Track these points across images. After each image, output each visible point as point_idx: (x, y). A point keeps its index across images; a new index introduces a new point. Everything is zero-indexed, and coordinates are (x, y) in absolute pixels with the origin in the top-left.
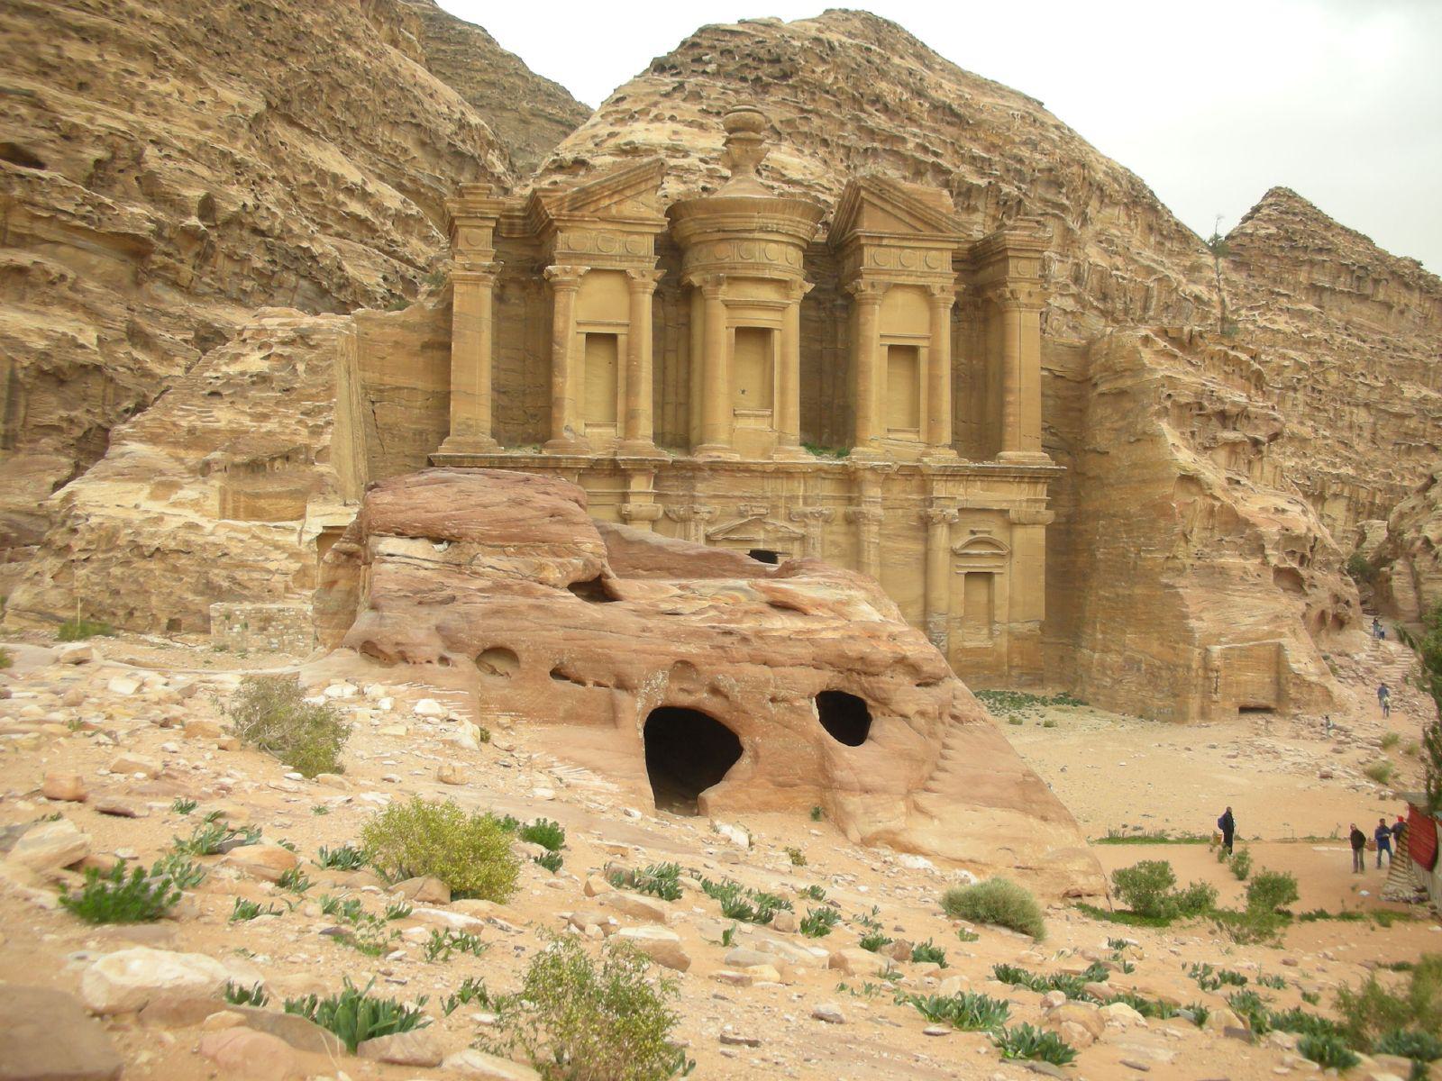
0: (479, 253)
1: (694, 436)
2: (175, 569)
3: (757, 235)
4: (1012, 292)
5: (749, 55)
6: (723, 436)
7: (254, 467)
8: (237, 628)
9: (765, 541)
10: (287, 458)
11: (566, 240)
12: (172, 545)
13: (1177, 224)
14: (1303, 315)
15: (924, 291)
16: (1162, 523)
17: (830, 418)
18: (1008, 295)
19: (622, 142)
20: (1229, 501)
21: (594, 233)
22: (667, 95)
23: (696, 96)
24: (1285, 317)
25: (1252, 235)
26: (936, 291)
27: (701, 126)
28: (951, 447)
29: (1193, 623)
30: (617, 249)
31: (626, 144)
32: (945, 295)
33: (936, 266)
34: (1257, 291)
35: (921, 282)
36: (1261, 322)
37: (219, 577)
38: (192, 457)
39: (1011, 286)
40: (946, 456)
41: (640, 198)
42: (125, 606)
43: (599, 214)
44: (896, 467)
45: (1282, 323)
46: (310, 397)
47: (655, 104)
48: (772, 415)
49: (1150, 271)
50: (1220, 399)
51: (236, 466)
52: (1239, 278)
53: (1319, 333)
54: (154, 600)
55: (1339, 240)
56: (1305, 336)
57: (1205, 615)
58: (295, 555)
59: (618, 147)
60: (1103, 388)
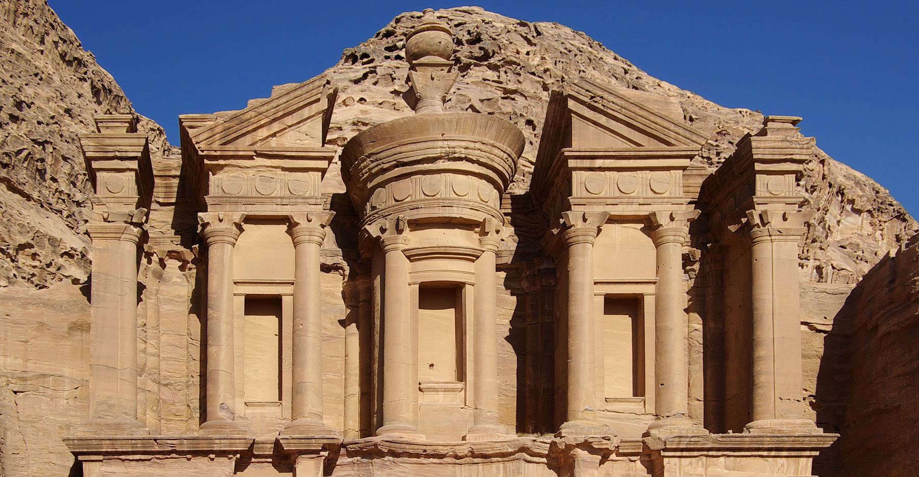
0: (120, 200)
3: (441, 165)
4: (761, 216)
11: (218, 182)
15: (650, 225)
18: (757, 220)
21: (251, 172)
26: (663, 220)
30: (278, 191)
32: (674, 225)
33: (671, 195)
35: (644, 211)
39: (759, 209)
41: (304, 127)
43: (256, 147)
44: (615, 442)
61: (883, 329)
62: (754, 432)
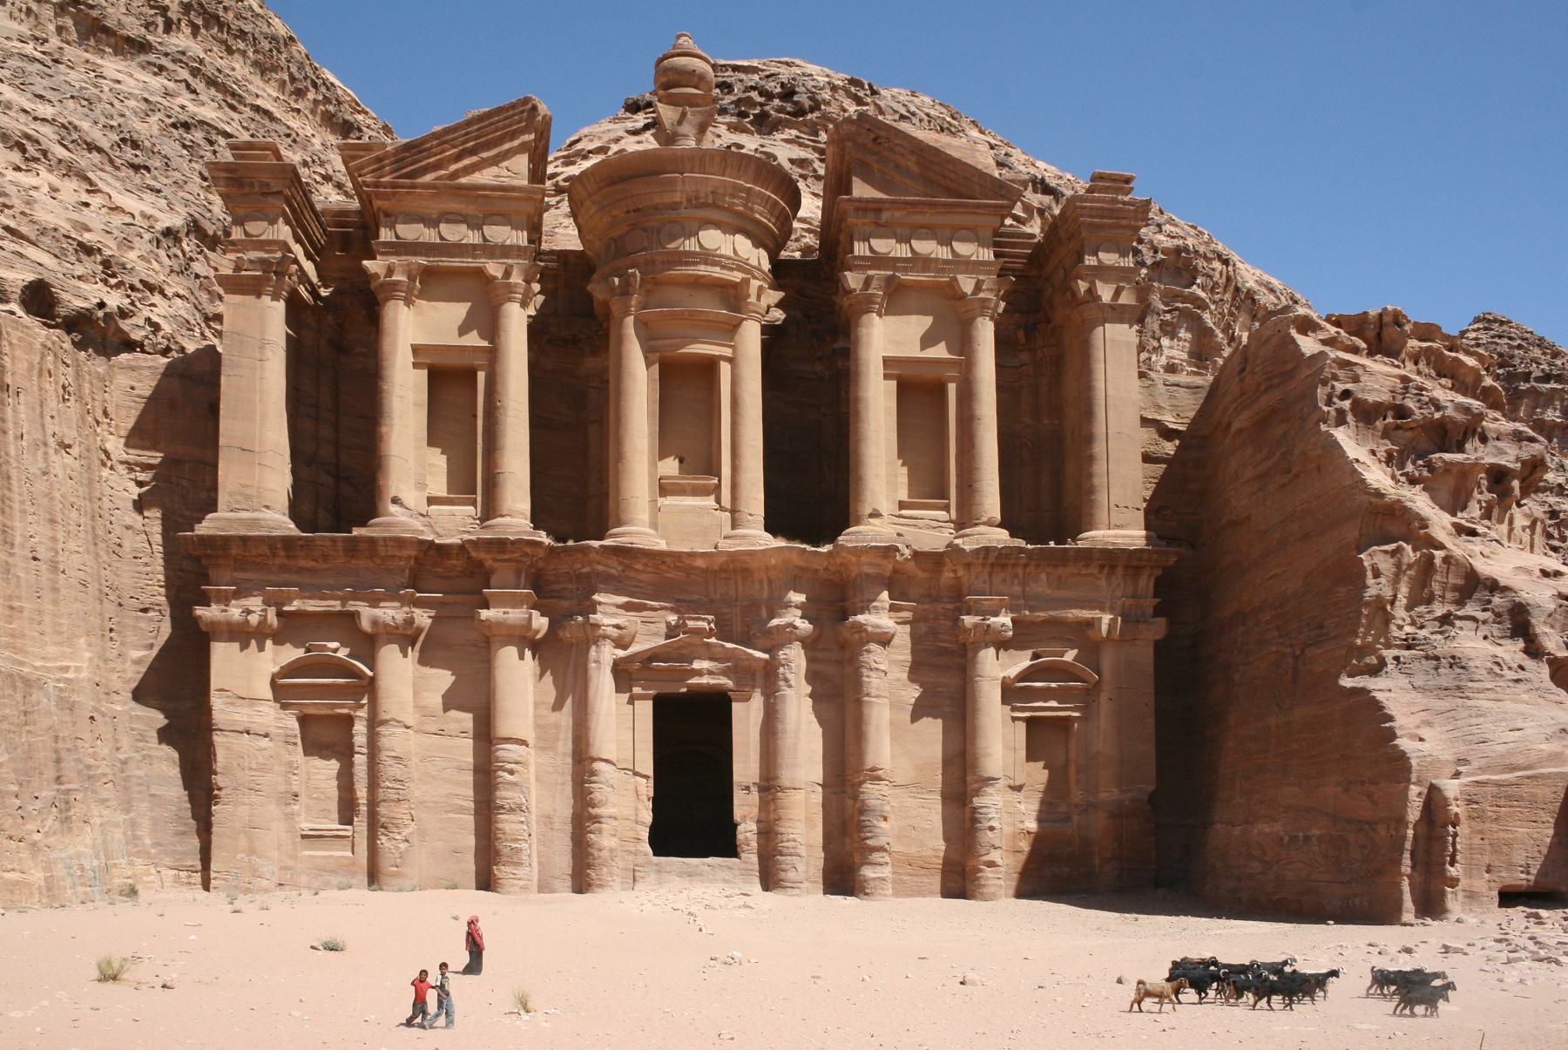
1: (612, 520)
5: (753, 88)
9: (710, 673)
17: (811, 487)
22: (635, 133)
28: (1000, 526)
29: (1404, 743)
47: (617, 140)
48: (719, 486)
57: (1424, 732)
61: (1236, 425)
62: (1080, 545)
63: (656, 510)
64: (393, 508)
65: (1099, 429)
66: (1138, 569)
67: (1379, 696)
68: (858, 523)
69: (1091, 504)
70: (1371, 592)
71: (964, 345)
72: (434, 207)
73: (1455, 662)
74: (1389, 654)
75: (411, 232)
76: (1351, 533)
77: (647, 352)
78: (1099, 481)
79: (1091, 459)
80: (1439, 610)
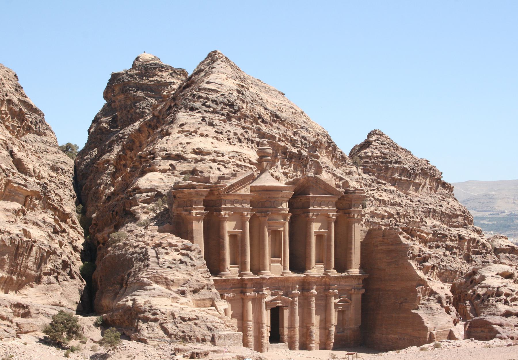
2: (196, 324)
6: (268, 268)
7: (195, 291)
8: (222, 340)
10: (202, 288)
12: (194, 317)
13: (341, 153)
14: (391, 192)
16: (412, 294)
19: (195, 148)
20: (430, 287)
23: (211, 124)
24: (384, 194)
25: (370, 156)
27: (217, 139)
28: (334, 269)
31: (197, 149)
34: (373, 182)
36: (377, 197)
37: (209, 325)
38: (175, 288)
40: (333, 273)
42: (188, 336)
45: (385, 196)
46: (201, 268)
49: (341, 179)
50: (425, 253)
51: (191, 291)
52: (365, 176)
53: (398, 200)
54: (196, 333)
55: (402, 155)
56: (392, 201)
58: (220, 318)
59: (194, 149)
60: (380, 248)
63: (270, 266)
64: (227, 270)
65: (353, 247)
66: (360, 278)
67: (420, 315)
68: (310, 269)
69: (351, 263)
70: (418, 296)
71: (329, 228)
72: (232, 198)
73: (431, 308)
74: (420, 306)
75: (229, 206)
76: (415, 284)
77: (268, 230)
78: (353, 258)
79: (351, 253)
80: (427, 297)
